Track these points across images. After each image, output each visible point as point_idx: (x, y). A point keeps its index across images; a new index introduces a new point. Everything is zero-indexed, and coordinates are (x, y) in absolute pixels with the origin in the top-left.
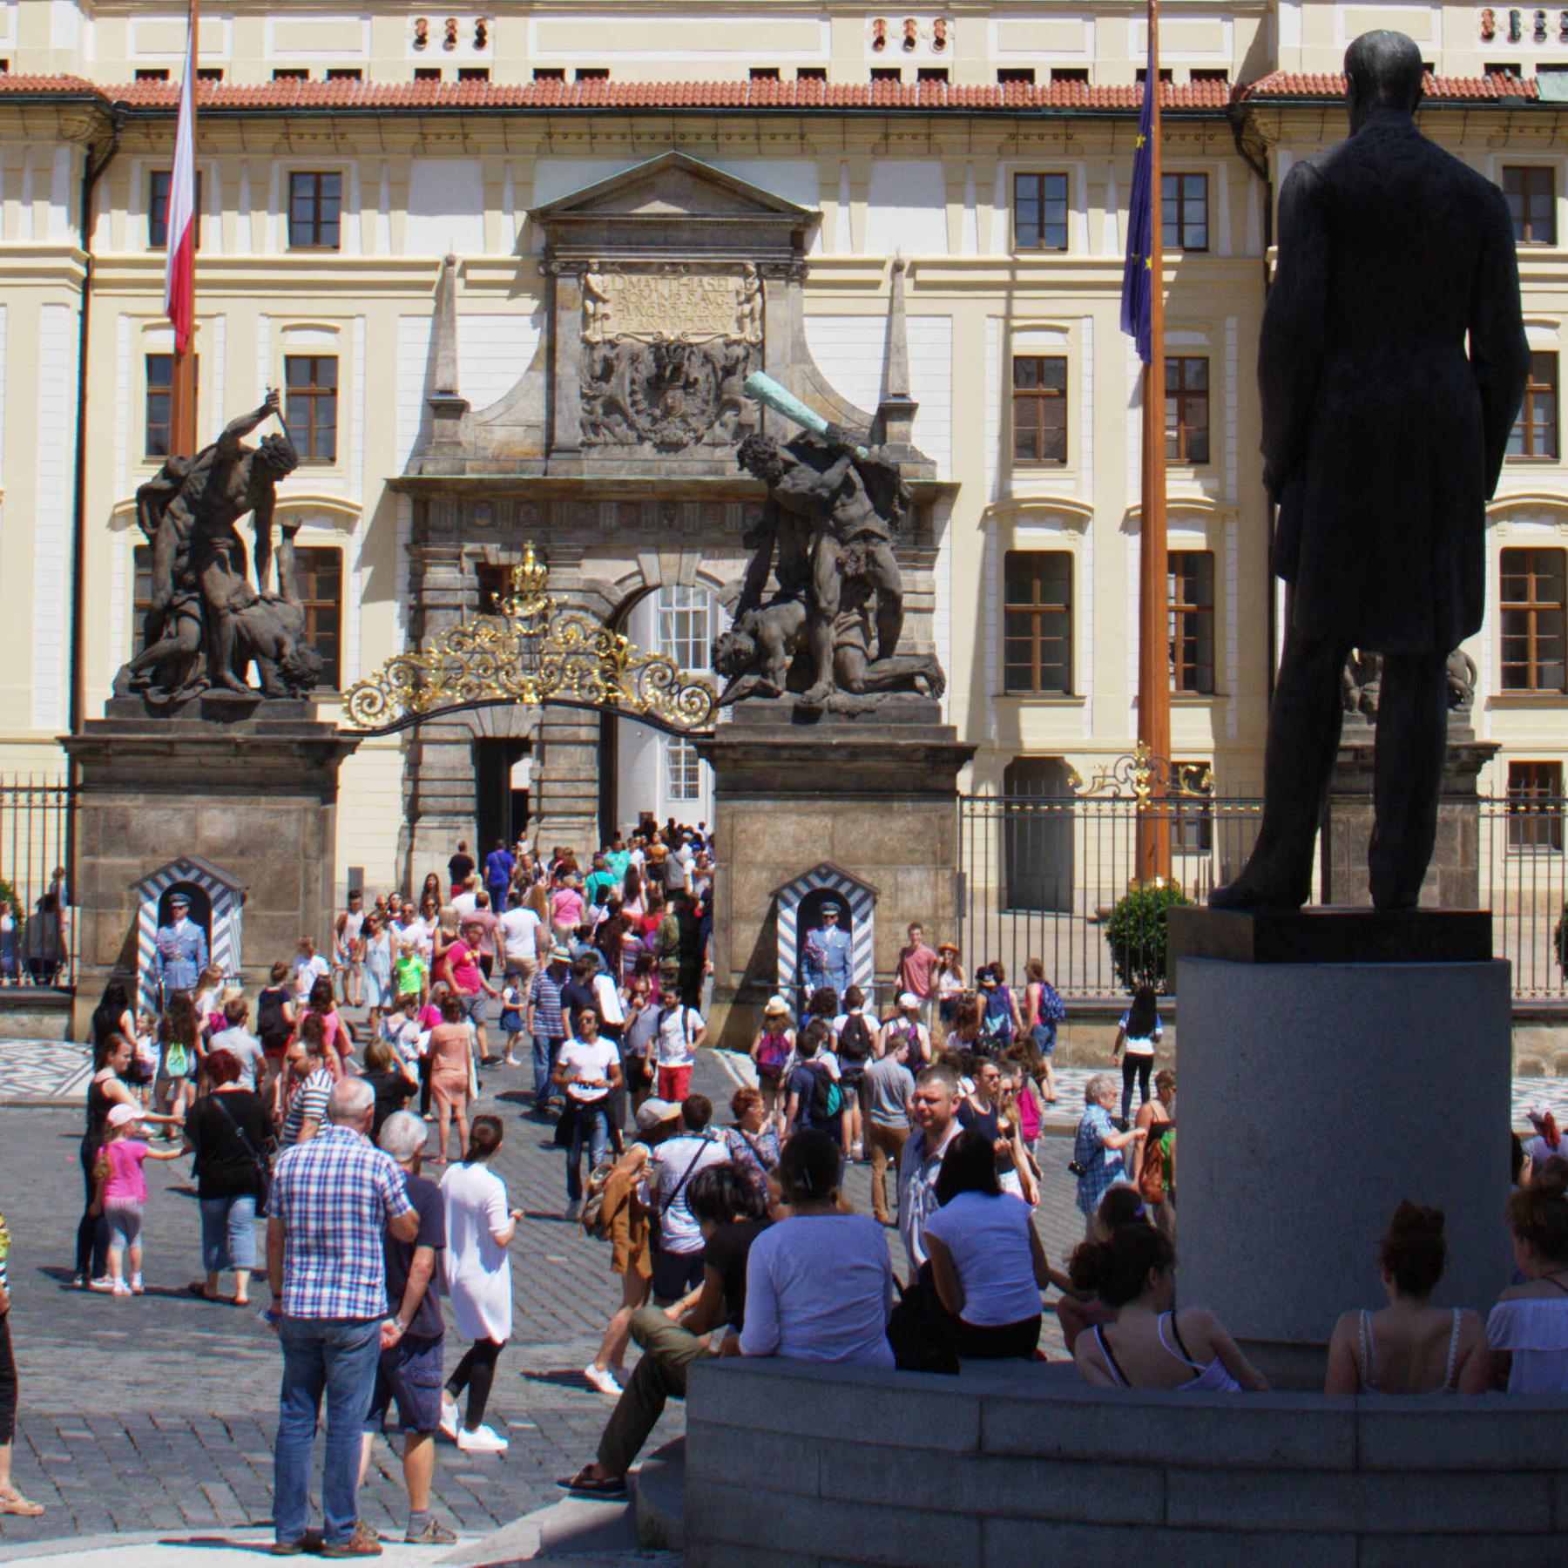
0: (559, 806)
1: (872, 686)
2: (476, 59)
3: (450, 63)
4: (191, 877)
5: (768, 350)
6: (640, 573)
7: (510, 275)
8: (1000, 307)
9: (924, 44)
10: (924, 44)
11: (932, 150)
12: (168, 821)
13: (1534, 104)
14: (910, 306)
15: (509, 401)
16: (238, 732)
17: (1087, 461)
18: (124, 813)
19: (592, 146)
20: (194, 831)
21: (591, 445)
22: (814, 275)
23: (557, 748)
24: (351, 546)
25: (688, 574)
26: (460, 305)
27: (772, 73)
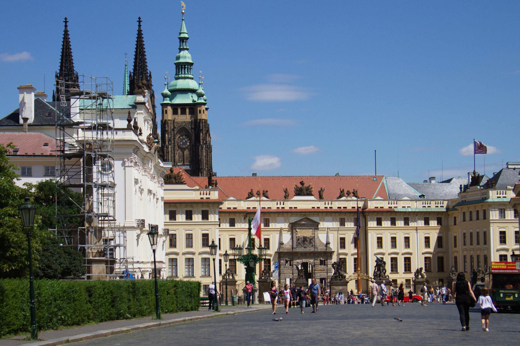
1: (384, 277)
3: (280, 207)
5: (315, 237)
7: (288, 229)
8: (337, 232)
9: (330, 204)
10: (330, 204)
11: (331, 216)
13: (394, 211)
14: (329, 232)
16: (342, 281)
17: (347, 248)
20: (339, 288)
21: (297, 247)
22: (319, 229)
24: (272, 259)
27: (314, 208)
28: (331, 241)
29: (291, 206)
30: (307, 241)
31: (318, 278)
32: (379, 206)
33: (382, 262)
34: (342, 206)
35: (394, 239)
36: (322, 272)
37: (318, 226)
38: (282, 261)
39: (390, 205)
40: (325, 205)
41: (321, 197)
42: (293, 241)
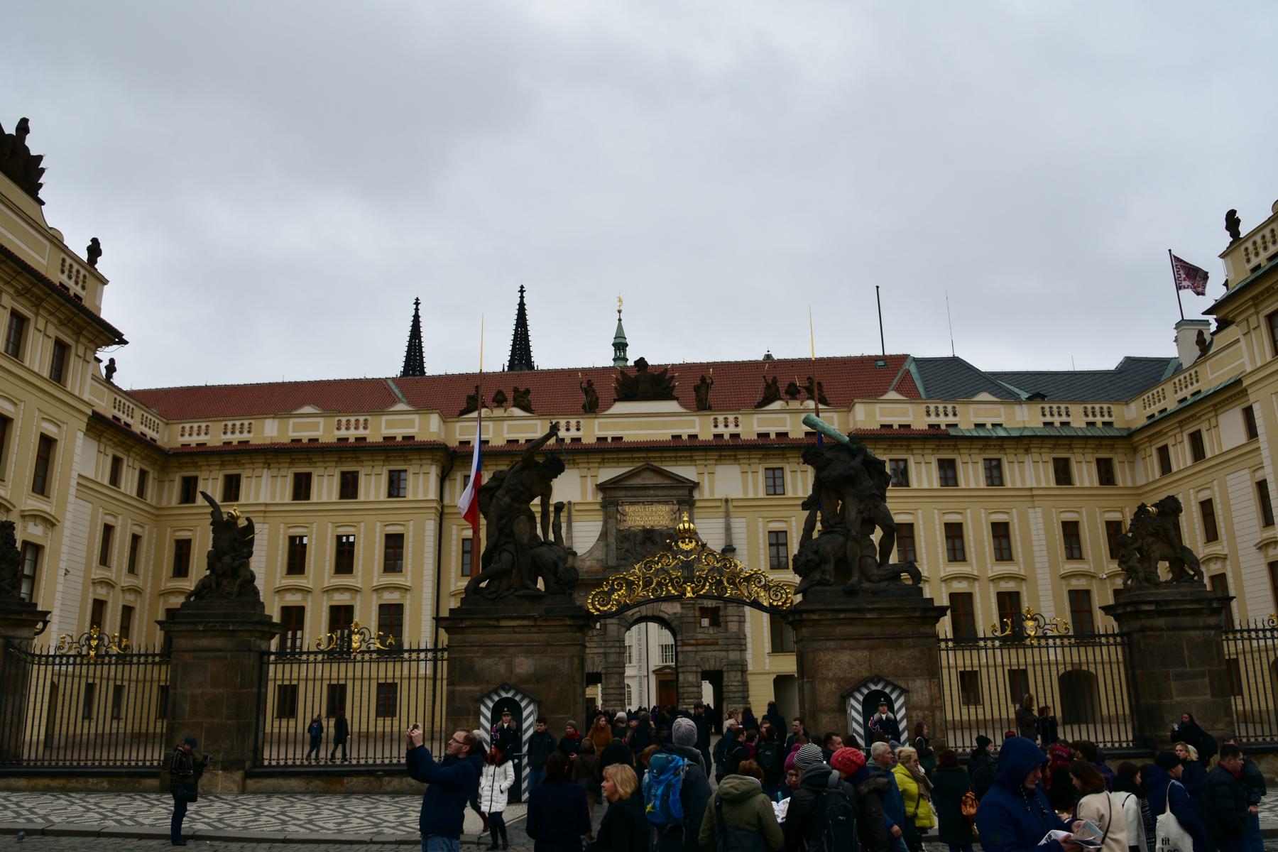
12: (496, 664)
13: (948, 437)
15: (591, 551)
19: (618, 461)
20: (510, 667)
22: (698, 504)
26: (574, 518)
27: (680, 436)
28: (740, 543)
29: (602, 434)
30: (654, 543)
31: (694, 669)
32: (896, 421)
33: (857, 462)
34: (773, 430)
35: (954, 532)
36: (708, 648)
37: (691, 495)
39: (933, 420)
40: (716, 426)
42: (607, 545)
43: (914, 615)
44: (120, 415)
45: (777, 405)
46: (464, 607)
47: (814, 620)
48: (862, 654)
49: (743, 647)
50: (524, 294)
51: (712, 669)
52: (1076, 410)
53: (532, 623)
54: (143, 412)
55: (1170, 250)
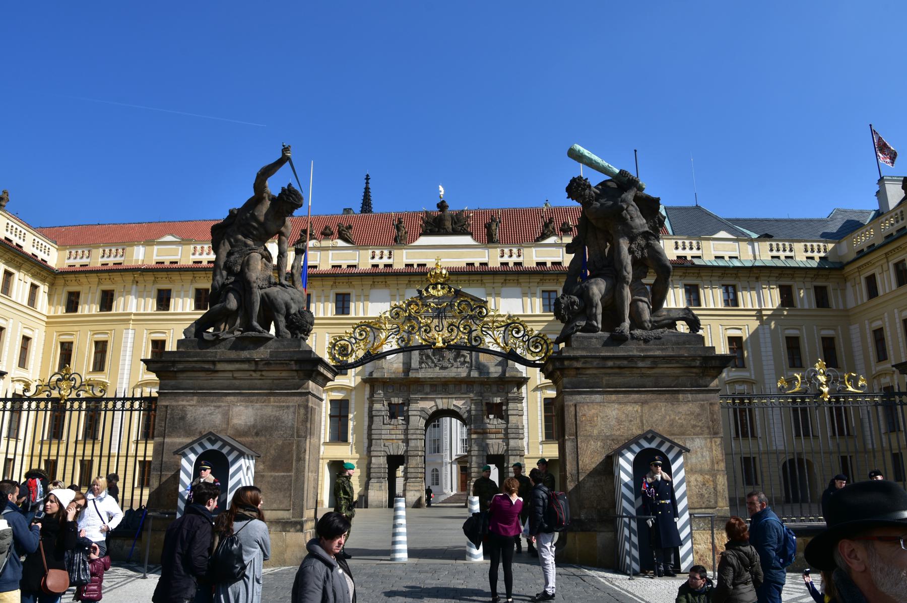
0: (413, 475)
1: (654, 327)
2: (390, 262)
3: (381, 263)
4: (216, 447)
6: (437, 405)
12: (211, 414)
13: (694, 266)
18: (183, 409)
21: (421, 368)
23: (412, 458)
25: (451, 406)
27: (473, 264)
29: (409, 262)
38: (377, 406)
39: (680, 252)
41: (490, 239)
43: (693, 364)
44: (11, 237)
45: (552, 240)
46: (180, 350)
47: (577, 369)
48: (633, 409)
49: (521, 436)
50: (369, 181)
51: (496, 453)
52: (799, 247)
53: (253, 368)
54: (35, 237)
55: (871, 125)
